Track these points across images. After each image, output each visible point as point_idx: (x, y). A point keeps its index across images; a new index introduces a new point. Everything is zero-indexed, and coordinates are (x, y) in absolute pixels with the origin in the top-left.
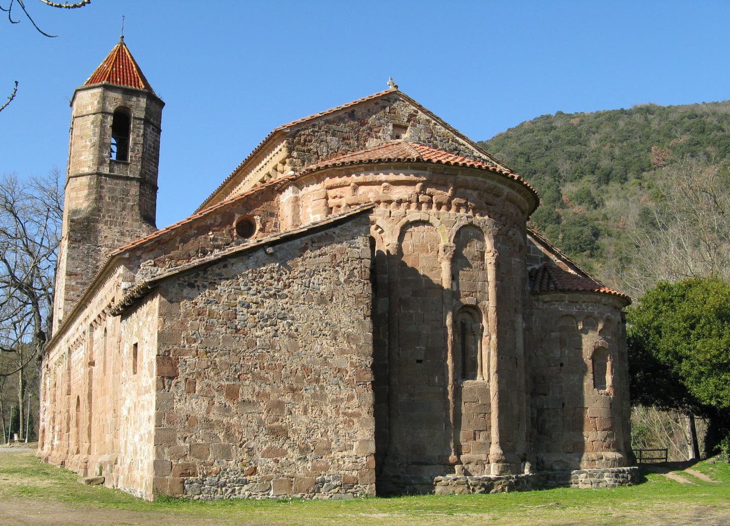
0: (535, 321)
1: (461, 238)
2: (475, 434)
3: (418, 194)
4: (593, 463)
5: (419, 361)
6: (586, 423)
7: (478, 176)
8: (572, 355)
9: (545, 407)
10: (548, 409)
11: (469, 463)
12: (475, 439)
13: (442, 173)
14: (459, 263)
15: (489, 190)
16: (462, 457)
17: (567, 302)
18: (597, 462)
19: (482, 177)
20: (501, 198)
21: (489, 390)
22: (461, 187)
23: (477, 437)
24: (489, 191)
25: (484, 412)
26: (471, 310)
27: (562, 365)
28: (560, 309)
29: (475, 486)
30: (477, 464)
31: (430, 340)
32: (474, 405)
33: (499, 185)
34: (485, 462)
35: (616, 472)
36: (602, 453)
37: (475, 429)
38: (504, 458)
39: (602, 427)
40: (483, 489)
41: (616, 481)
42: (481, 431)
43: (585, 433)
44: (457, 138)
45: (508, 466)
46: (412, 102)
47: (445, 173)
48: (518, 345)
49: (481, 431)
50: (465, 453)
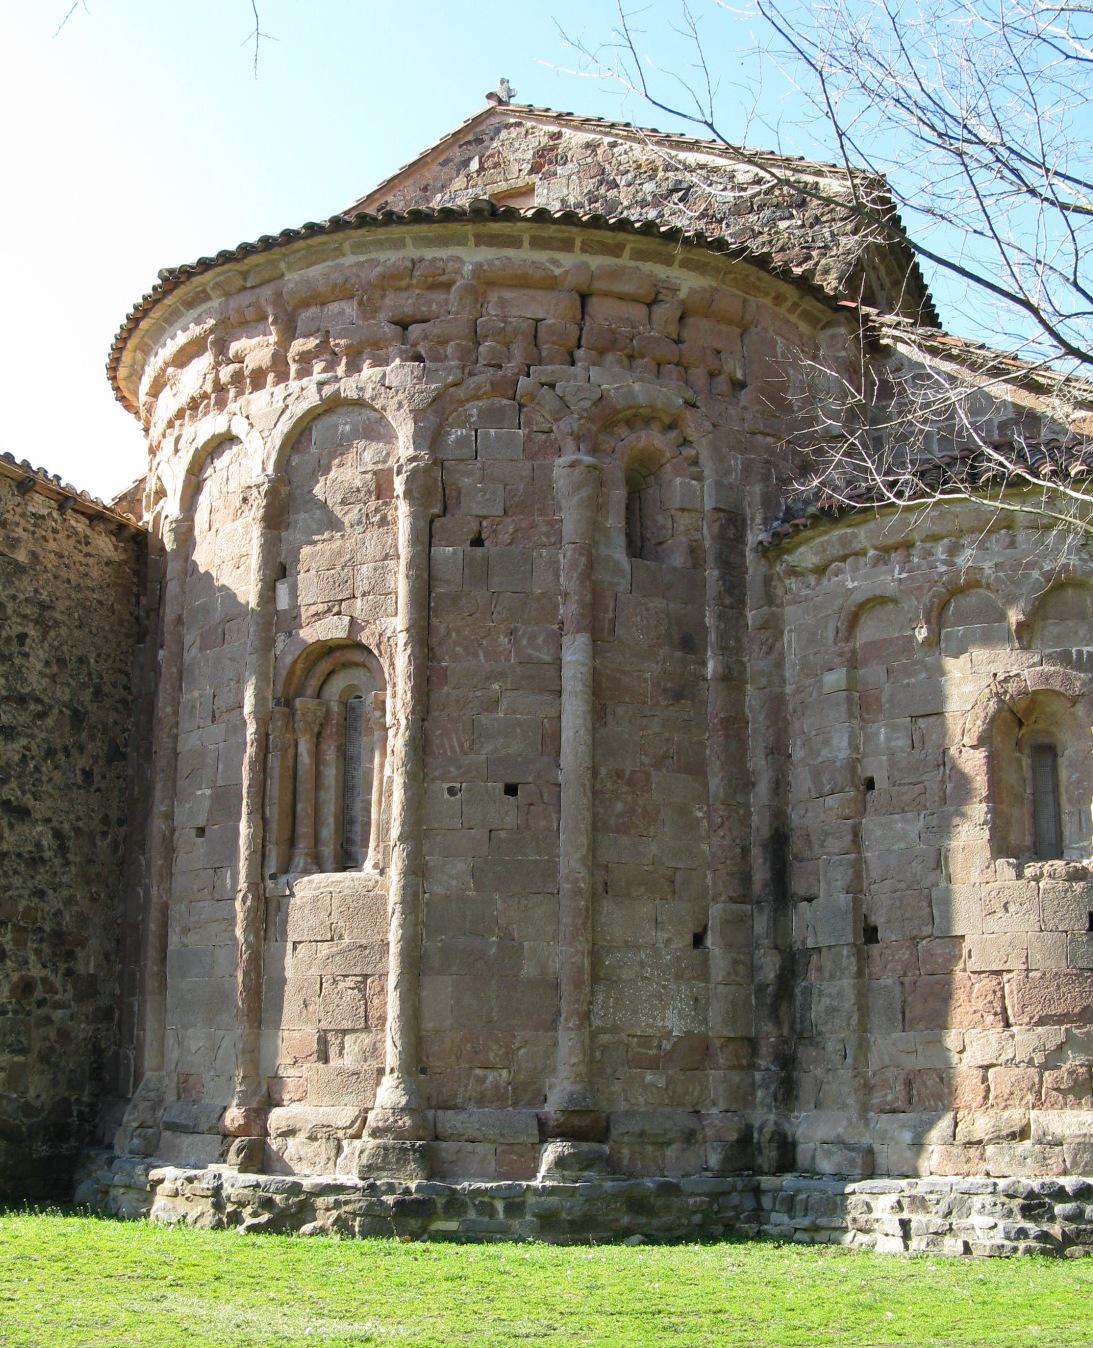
0: (790, 642)
1: (313, 449)
2: (323, 1042)
3: (217, 365)
4: (973, 1152)
5: (201, 831)
6: (960, 996)
7: (339, 252)
8: (900, 743)
9: (810, 943)
10: (819, 950)
11: (290, 1132)
12: (324, 1058)
13: (245, 288)
14: (300, 524)
15: (391, 280)
16: (277, 1118)
17: (871, 553)
18: (990, 1150)
19: (353, 253)
20: (453, 289)
21: (384, 899)
22: (305, 304)
23: (333, 1051)
24: (403, 283)
25: (357, 971)
26: (357, 656)
27: (870, 784)
28: (850, 585)
29: (242, 1204)
30: (312, 1138)
31: (221, 766)
32: (324, 949)
33: (429, 254)
34: (340, 1134)
35: (1031, 1195)
36: (1033, 1114)
37: (324, 1025)
38: (406, 1121)
39: (1037, 1011)
40: (265, 1217)
41: (1022, 1233)
42: (345, 1032)
43: (952, 1040)
44: (682, 155)
45: (404, 1150)
46: (544, 115)
47: (249, 285)
48: (567, 736)
49: (345, 1032)
50: (292, 1101)
